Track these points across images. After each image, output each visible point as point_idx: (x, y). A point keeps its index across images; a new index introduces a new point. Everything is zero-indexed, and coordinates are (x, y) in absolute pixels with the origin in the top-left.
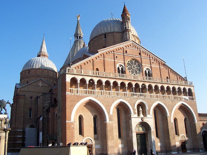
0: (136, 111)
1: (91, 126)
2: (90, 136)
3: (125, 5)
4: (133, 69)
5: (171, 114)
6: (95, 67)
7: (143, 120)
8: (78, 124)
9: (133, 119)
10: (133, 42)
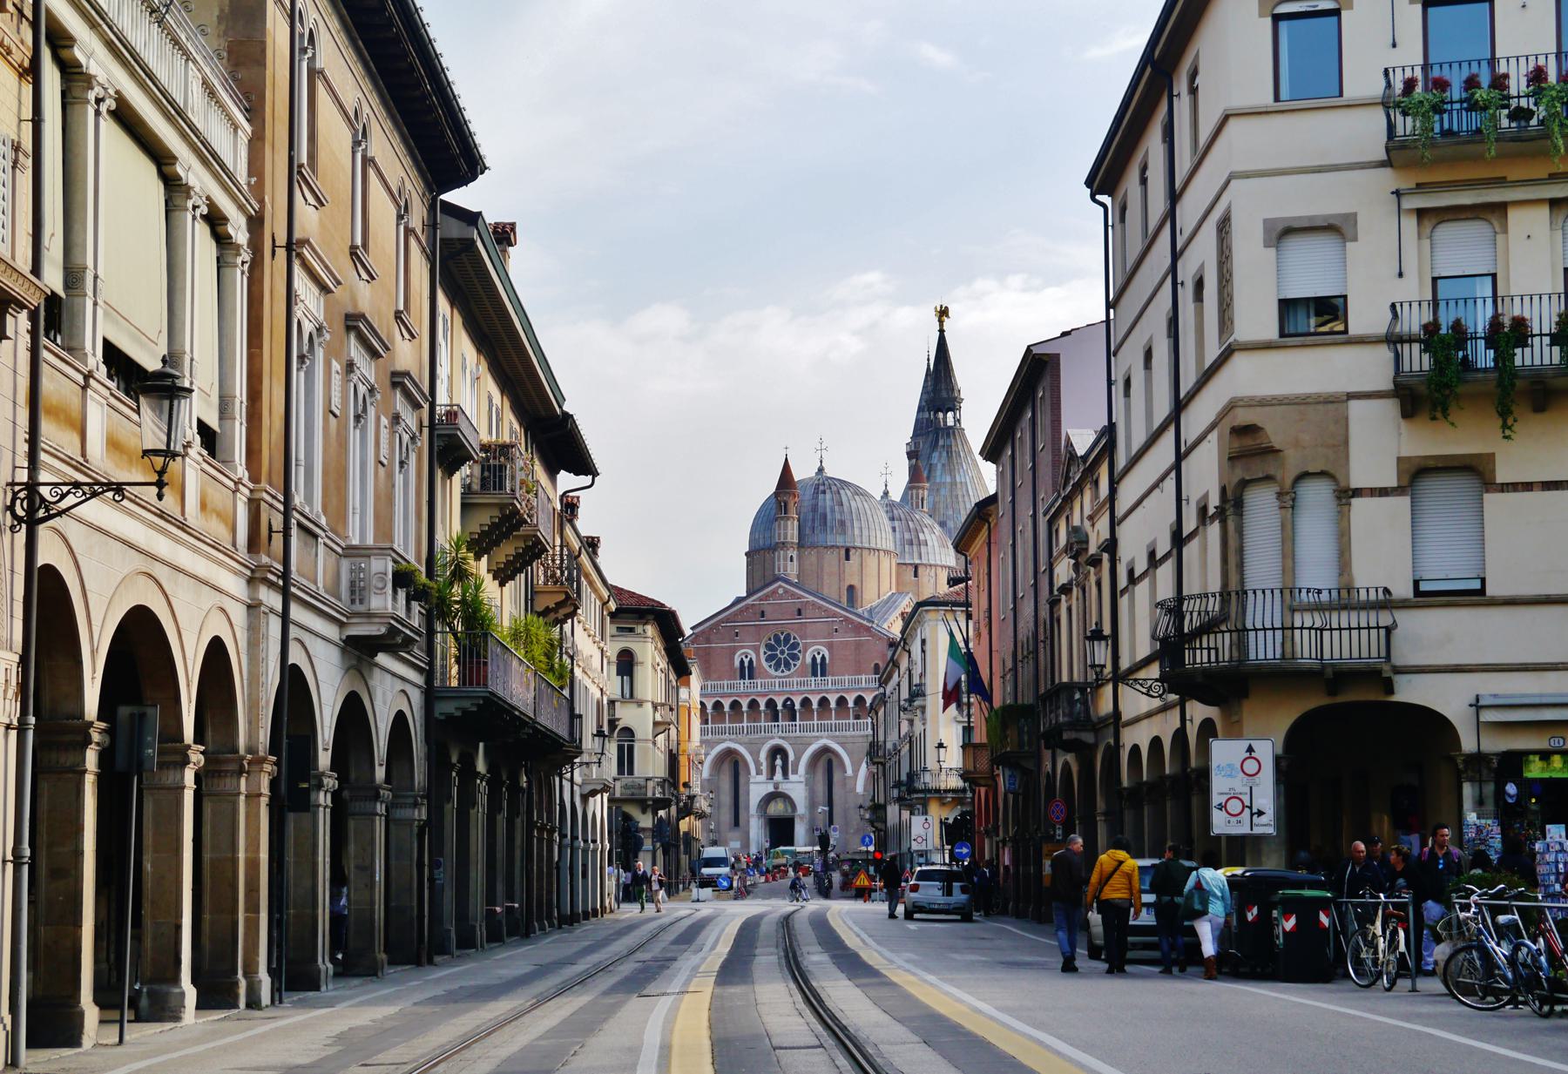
0: (764, 768)
3: (786, 459)
9: (752, 787)
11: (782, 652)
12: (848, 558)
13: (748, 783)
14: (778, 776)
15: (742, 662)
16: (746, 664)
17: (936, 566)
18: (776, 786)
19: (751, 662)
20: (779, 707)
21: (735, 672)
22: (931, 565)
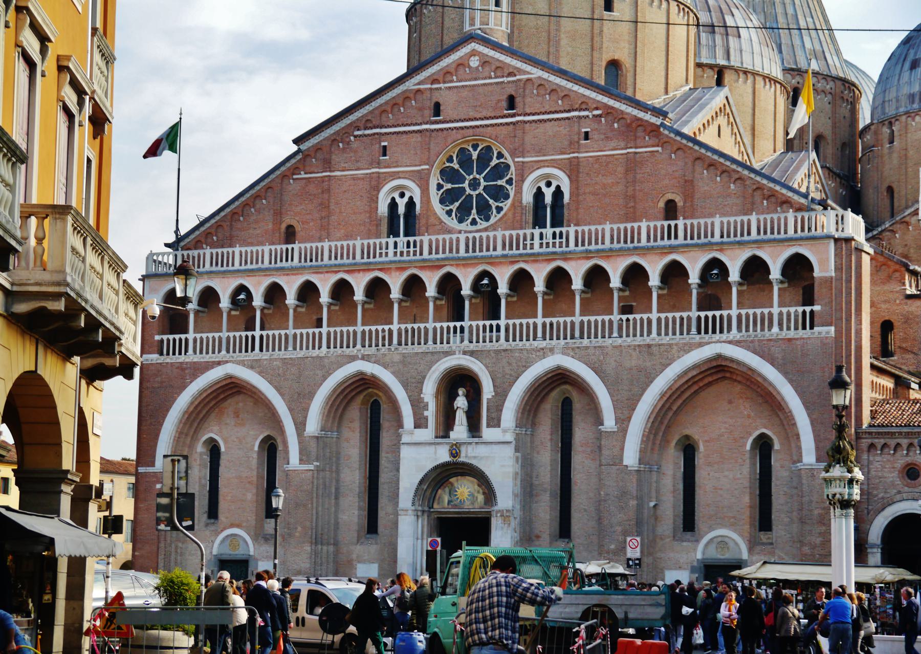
0: (431, 413)
1: (249, 482)
2: (244, 524)
4: (470, 196)
5: (629, 418)
9: (406, 453)
11: (474, 184)
13: (397, 445)
14: (460, 431)
15: (393, 205)
16: (401, 210)
17: (755, 74)
18: (454, 453)
19: (411, 204)
20: (466, 291)
21: (378, 225)
22: (745, 72)
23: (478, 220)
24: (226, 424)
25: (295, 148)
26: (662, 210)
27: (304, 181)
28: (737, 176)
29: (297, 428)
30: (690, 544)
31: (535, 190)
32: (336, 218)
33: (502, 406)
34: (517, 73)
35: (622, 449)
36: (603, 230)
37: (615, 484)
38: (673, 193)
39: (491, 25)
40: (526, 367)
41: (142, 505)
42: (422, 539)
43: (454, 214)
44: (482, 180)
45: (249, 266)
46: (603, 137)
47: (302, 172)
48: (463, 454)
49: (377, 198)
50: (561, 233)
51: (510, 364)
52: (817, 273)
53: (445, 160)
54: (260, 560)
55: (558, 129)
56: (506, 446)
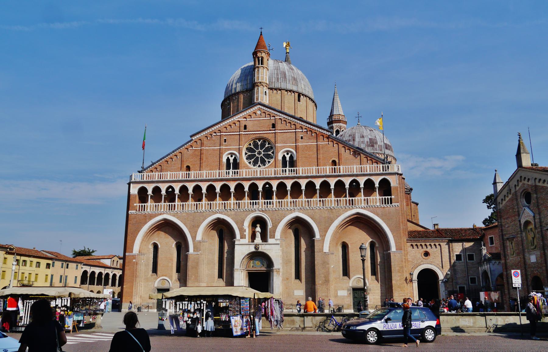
0: (248, 233)
3: (261, 34)
4: (258, 157)
5: (325, 235)
6: (183, 165)
7: (257, 250)
8: (151, 257)
9: (237, 247)
10: (261, 107)
11: (259, 153)
12: (299, 100)
15: (228, 160)
16: (231, 161)
20: (260, 189)
23: (261, 165)
24: (161, 237)
25: (190, 139)
26: (331, 163)
27: (194, 150)
28: (358, 153)
29: (192, 239)
30: (347, 281)
31: (283, 156)
32: (206, 163)
33: (276, 231)
34: (275, 116)
35: (323, 246)
36: (313, 169)
37: (320, 259)
38: (335, 158)
39: (264, 101)
40: (285, 217)
41: (127, 268)
42: (243, 280)
43: (251, 163)
44: (262, 152)
45: (173, 179)
46: (308, 138)
47: (193, 147)
48: (260, 248)
49: (222, 157)
50: (294, 170)
51: (278, 215)
52: (392, 185)
53: (248, 145)
54: (174, 289)
55: (291, 135)
56: (277, 245)
